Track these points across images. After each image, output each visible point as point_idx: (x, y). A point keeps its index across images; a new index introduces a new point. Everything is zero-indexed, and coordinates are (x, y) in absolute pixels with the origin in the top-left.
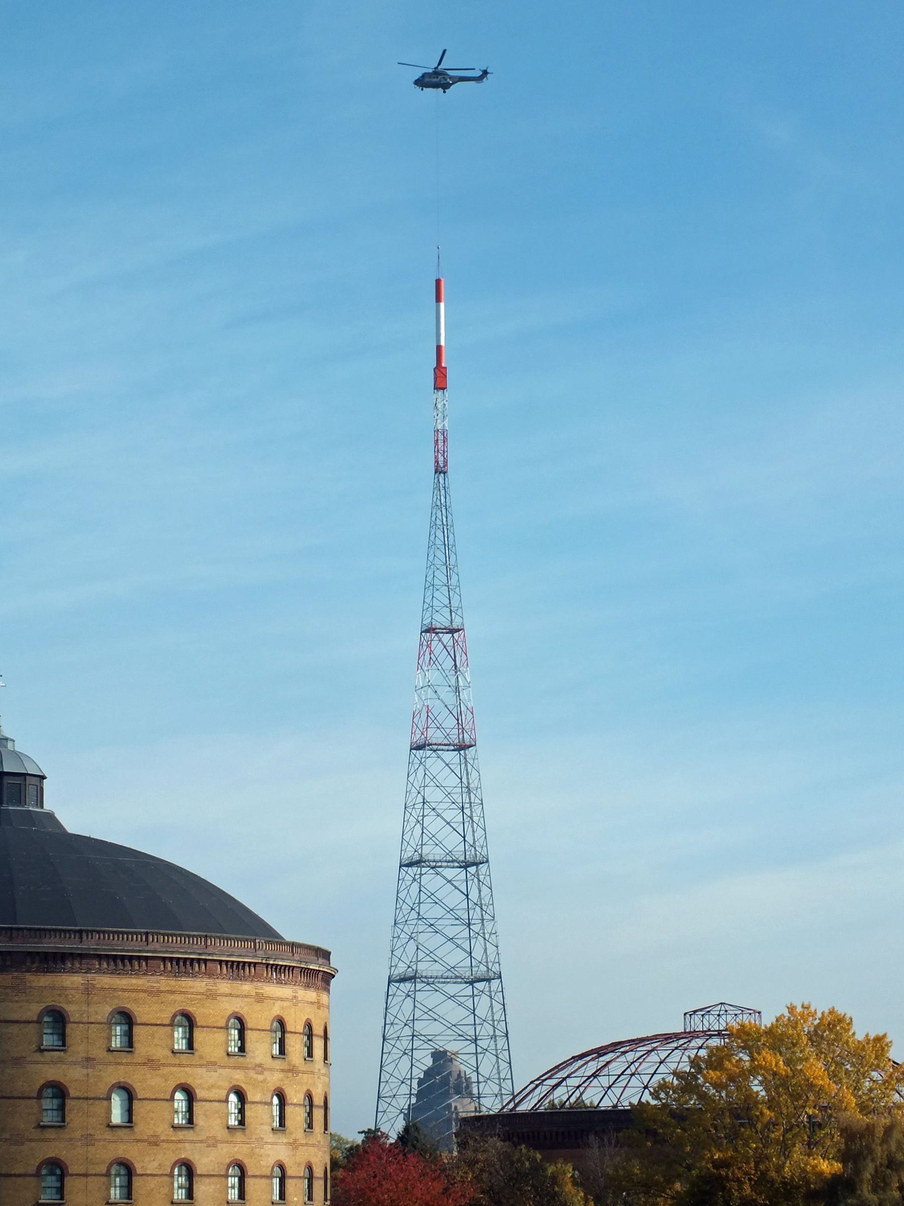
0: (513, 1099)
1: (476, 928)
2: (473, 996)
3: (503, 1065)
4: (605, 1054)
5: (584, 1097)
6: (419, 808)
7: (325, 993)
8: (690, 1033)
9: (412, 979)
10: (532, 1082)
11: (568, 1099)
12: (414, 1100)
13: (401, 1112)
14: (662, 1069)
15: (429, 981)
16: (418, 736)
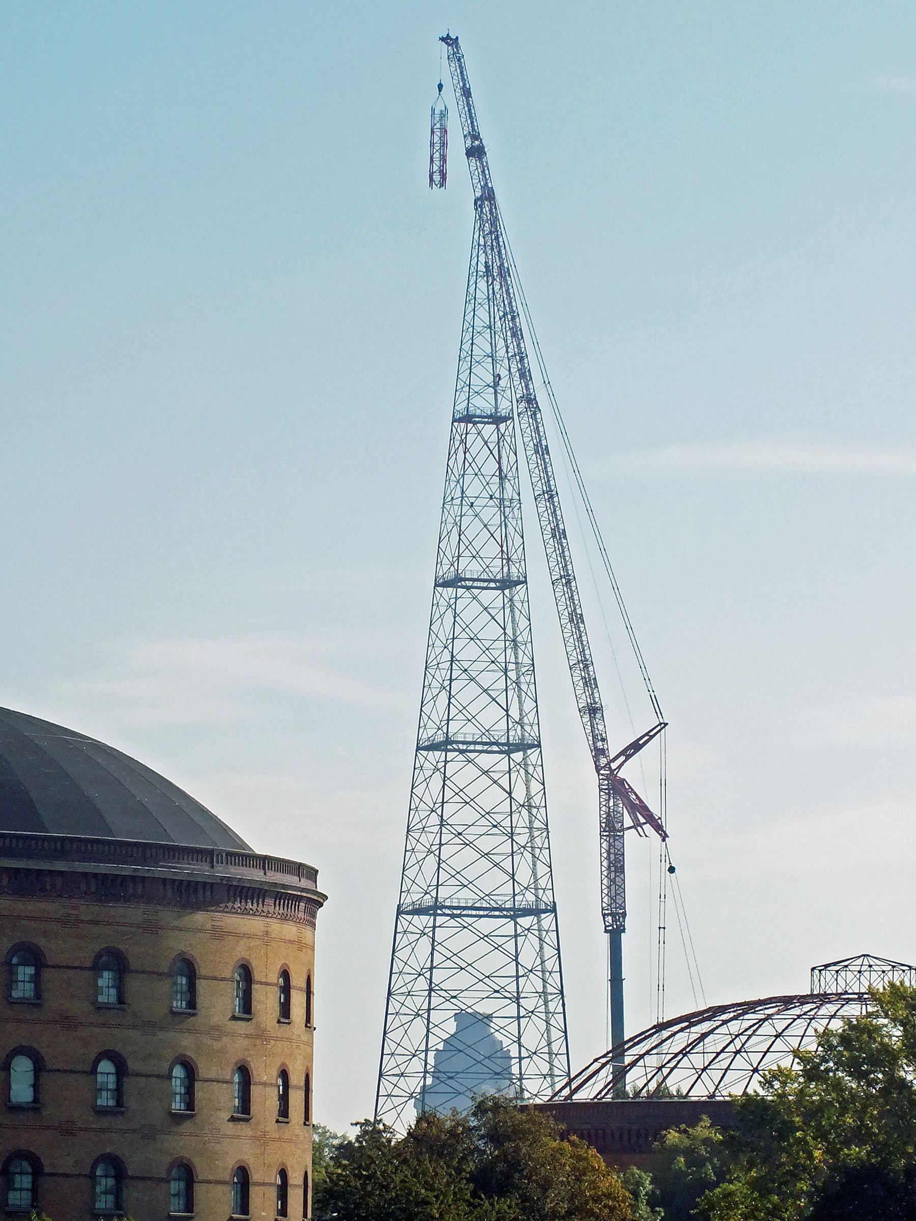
0: (568, 1084)
1: (522, 839)
2: (519, 1018)
6: (445, 672)
7: (308, 927)
8: (818, 995)
9: (434, 909)
10: (596, 1060)
11: (646, 1084)
12: (429, 1081)
13: (411, 1097)
14: (779, 1045)
15: (457, 912)
16: (446, 568)
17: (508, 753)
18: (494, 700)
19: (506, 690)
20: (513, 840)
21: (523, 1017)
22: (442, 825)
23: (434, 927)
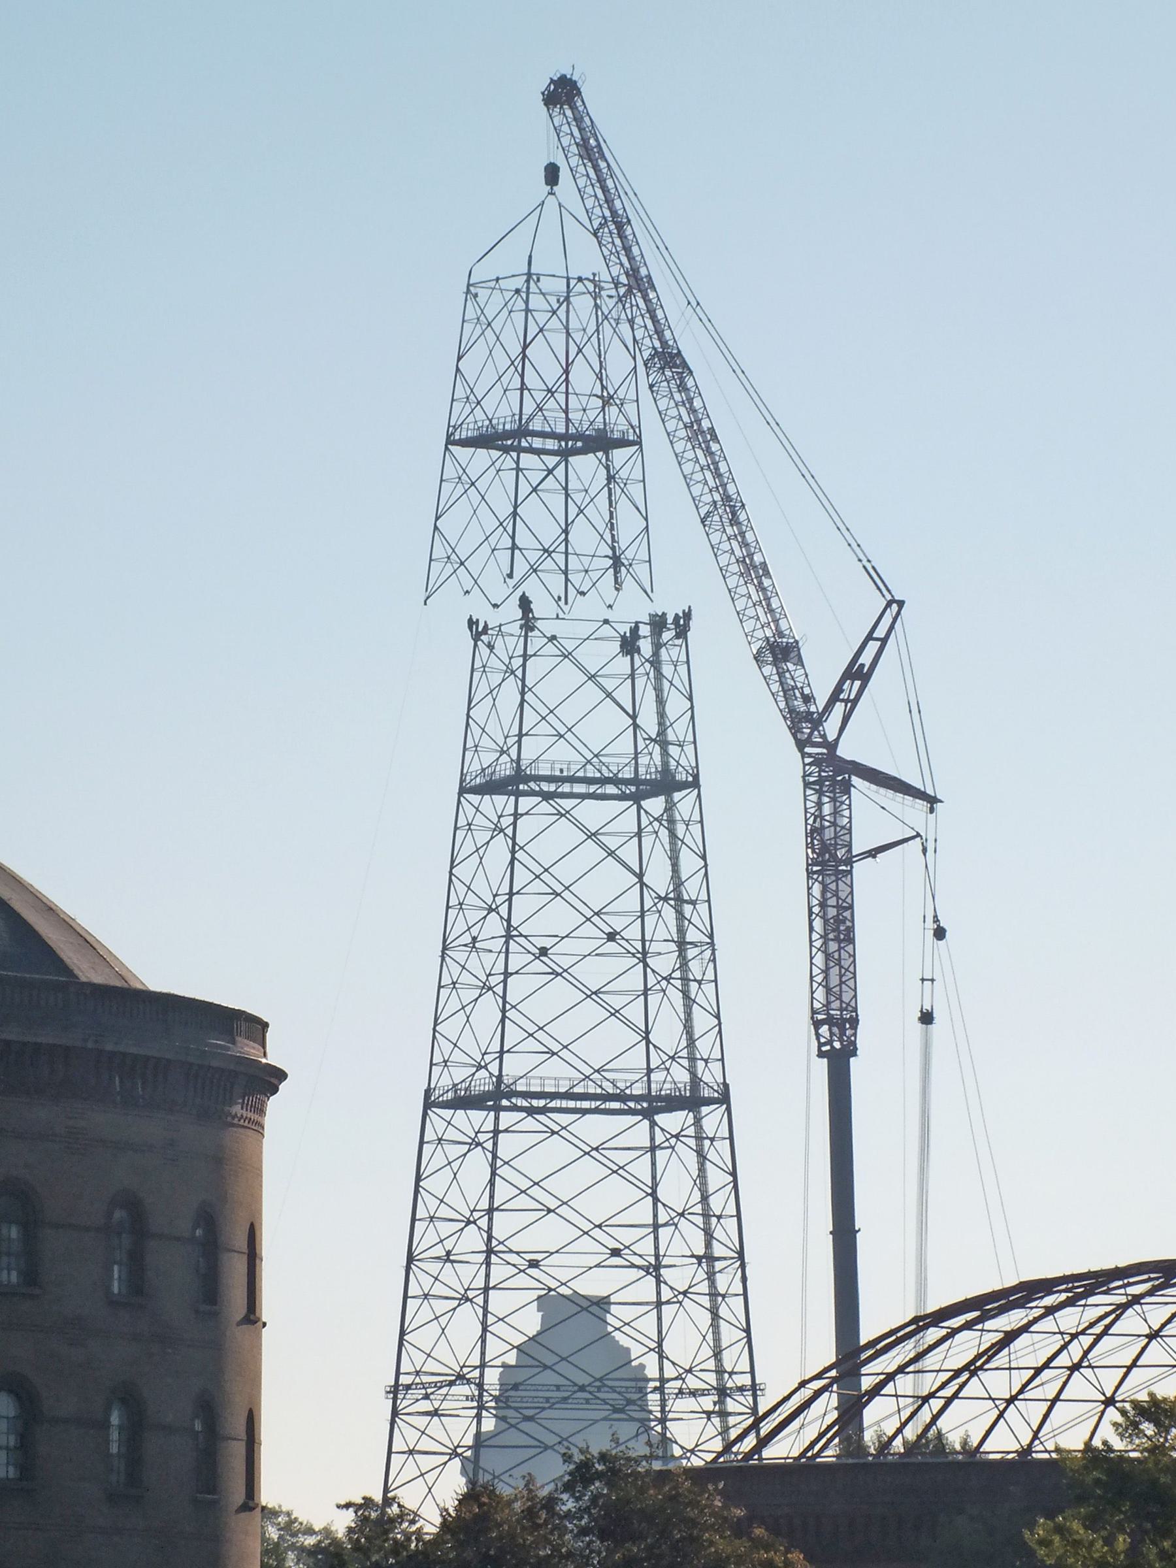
0: (755, 1426)
4: (1002, 1310)
5: (943, 1423)
10: (803, 1384)
11: (899, 1431)
12: (489, 1424)
15: (539, 1103)
17: (637, 798)
18: (609, 695)
19: (632, 676)
20: (646, 965)
21: (668, 1302)
22: (508, 937)
23: (496, 1132)
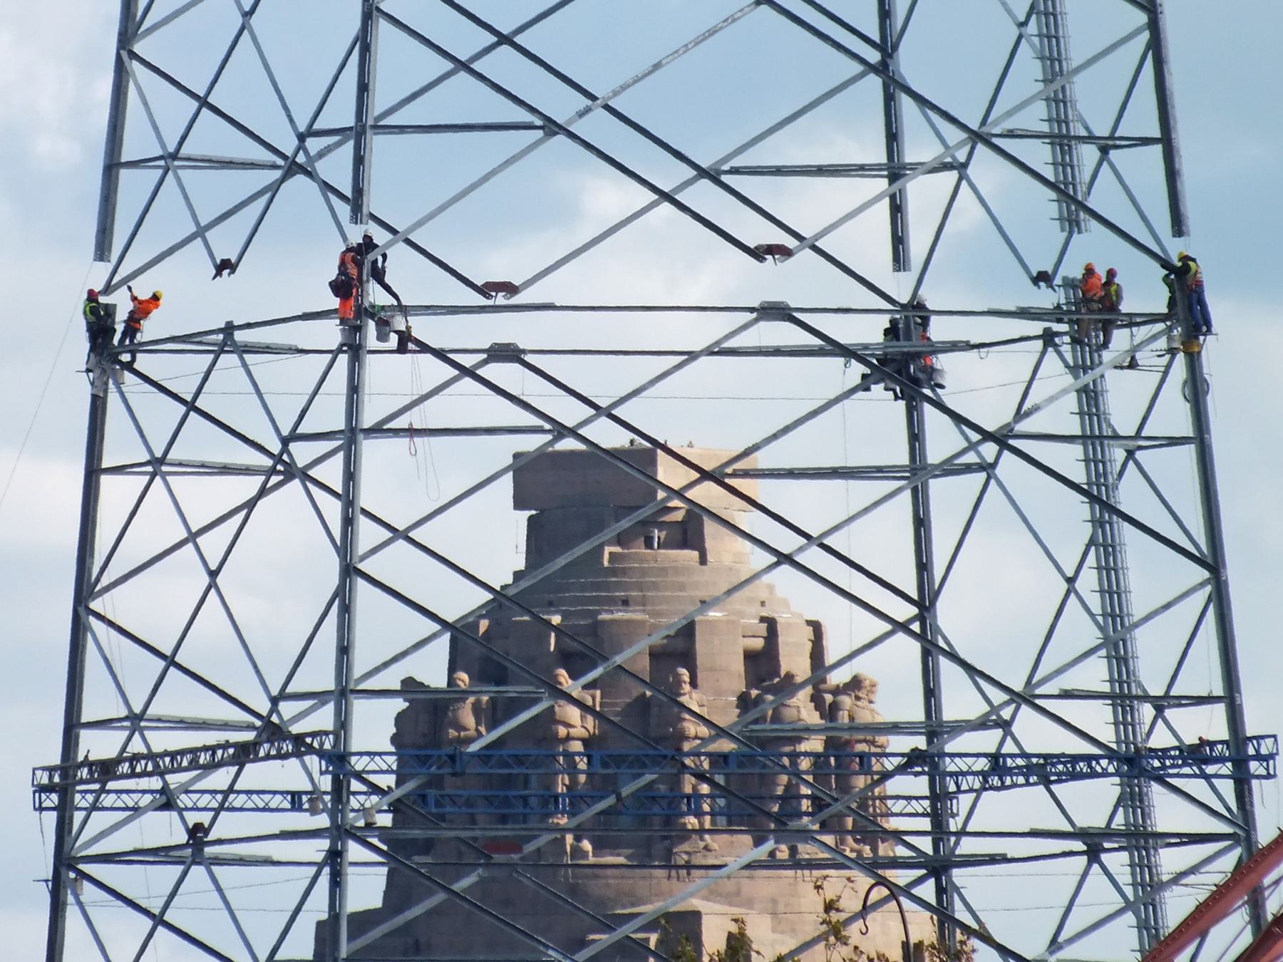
2: (917, 473)
3: (1154, 575)
12: (367, 888)
